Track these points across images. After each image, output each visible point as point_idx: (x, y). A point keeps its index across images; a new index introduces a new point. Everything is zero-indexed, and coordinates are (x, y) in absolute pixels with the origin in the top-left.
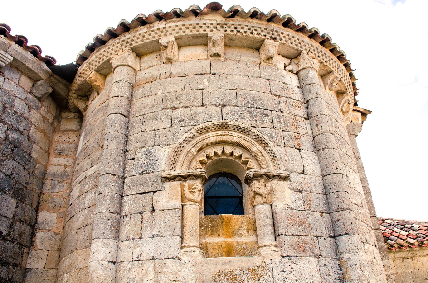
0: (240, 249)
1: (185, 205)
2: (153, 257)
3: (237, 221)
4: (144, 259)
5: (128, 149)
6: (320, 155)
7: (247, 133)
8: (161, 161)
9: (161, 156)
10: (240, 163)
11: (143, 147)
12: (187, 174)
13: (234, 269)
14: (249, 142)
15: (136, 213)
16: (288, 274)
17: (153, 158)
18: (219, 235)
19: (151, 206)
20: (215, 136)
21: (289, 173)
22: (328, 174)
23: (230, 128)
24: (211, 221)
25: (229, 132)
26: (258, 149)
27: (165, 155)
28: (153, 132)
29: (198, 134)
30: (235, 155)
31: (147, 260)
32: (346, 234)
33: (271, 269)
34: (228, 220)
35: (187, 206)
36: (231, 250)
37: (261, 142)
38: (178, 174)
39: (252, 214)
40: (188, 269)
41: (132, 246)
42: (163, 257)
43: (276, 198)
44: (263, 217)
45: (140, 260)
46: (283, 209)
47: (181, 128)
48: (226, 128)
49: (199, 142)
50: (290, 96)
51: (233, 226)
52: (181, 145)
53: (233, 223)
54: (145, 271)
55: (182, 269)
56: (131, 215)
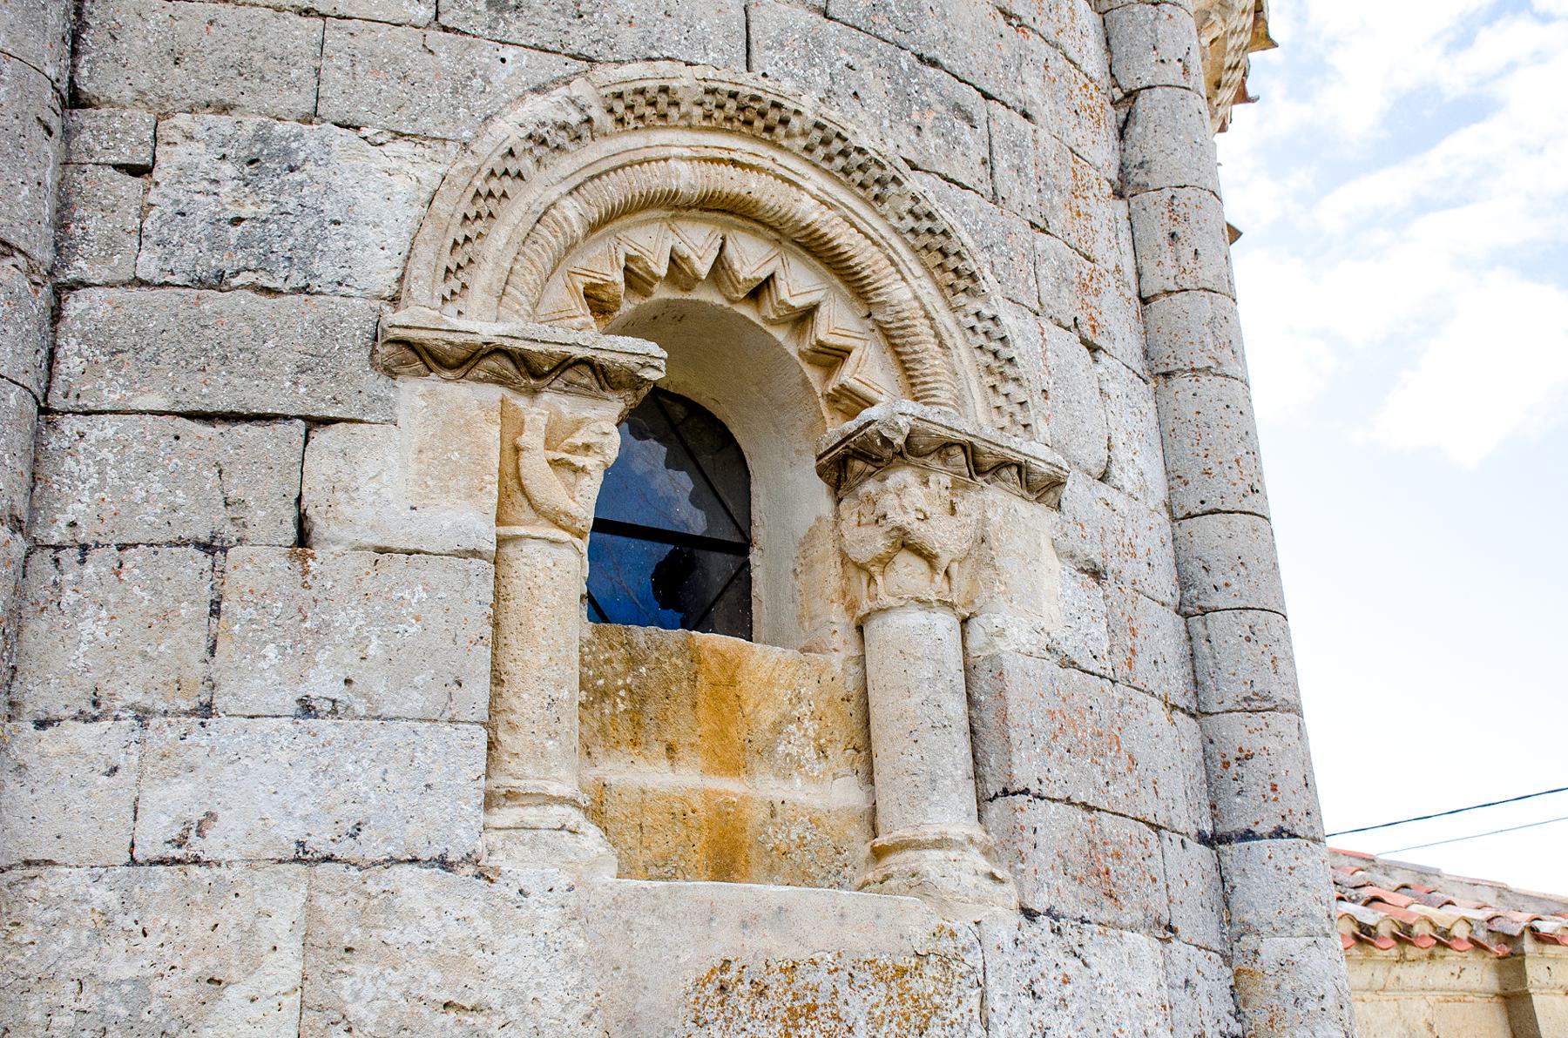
0: (783, 848)
1: (516, 539)
2: (301, 844)
3: (770, 683)
4: (226, 856)
5: (87, 87)
6: (1174, 405)
7: (876, 189)
8: (371, 235)
9: (369, 201)
10: (795, 354)
11: (225, 109)
12: (557, 349)
13: (805, 955)
14: (874, 243)
15: (170, 544)
16: (1051, 1011)
17: (309, 201)
18: (670, 749)
19: (290, 515)
20: (700, 159)
21: (1066, 467)
22: (1211, 512)
23: (788, 135)
24: (633, 662)
25: (782, 158)
26: (916, 298)
27: (399, 199)
28: (303, 21)
29: (609, 121)
30: (781, 302)
31: (251, 862)
32: (1279, 833)
33: (980, 976)
34: (723, 668)
35: (529, 548)
36: (736, 847)
37: (939, 259)
38: (498, 341)
39: (842, 655)
40: (539, 935)
41: (135, 759)
42: (373, 846)
43: (1003, 588)
44: (932, 682)
45: (197, 861)
46: (1030, 655)
47: (509, 53)
48: (769, 129)
49: (607, 173)
50: (1062, 39)
51: (747, 710)
52: (512, 165)
53: (749, 685)
54: (235, 935)
55: (501, 934)
56: (122, 547)
